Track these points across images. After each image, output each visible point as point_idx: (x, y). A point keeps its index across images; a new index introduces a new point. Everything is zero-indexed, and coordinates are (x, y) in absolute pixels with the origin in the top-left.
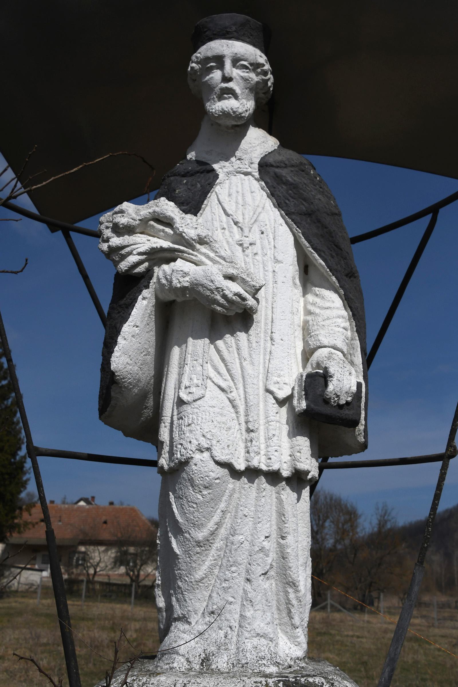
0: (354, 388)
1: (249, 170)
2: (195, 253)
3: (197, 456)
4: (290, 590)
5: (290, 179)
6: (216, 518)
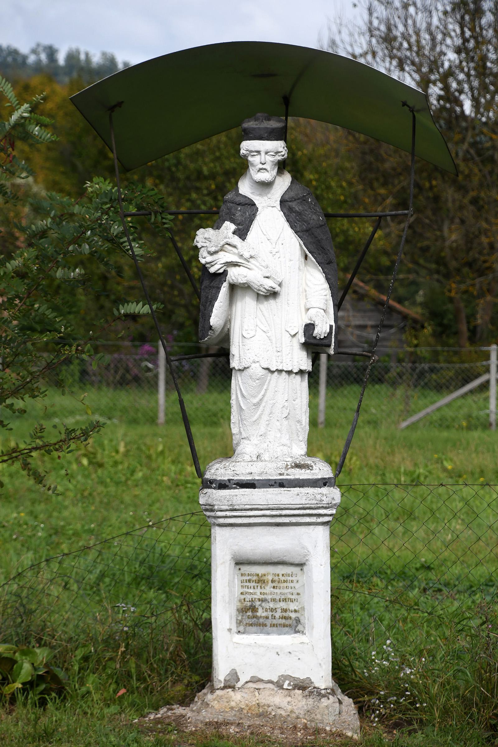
0: (328, 331)
1: (275, 205)
2: (249, 264)
3: (253, 365)
4: (298, 424)
5: (297, 209)
6: (262, 393)
